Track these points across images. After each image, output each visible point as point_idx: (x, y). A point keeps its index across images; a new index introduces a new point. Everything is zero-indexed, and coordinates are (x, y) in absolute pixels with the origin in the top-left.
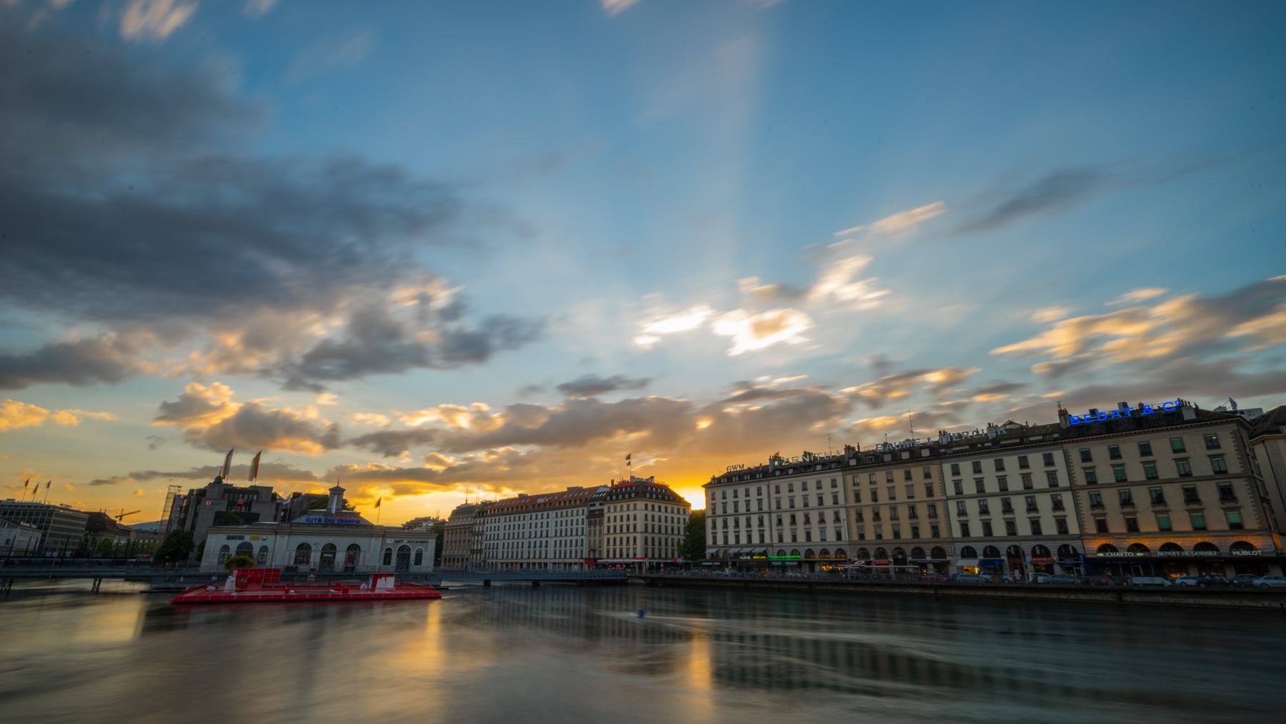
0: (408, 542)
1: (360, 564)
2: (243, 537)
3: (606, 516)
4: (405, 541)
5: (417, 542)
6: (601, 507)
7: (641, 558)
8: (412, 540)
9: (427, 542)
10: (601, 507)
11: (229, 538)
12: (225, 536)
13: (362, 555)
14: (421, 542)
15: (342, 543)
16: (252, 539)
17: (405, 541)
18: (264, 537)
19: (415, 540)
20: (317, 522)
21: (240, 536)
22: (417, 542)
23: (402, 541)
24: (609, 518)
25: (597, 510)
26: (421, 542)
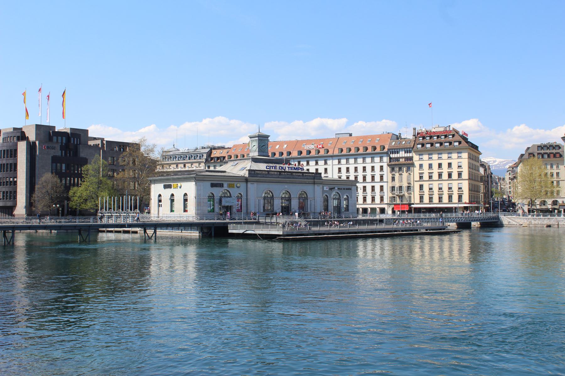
0: (339, 189)
1: (309, 211)
2: (223, 184)
3: (417, 164)
4: (336, 188)
5: (344, 189)
6: (409, 155)
7: (465, 203)
8: (340, 187)
9: (351, 189)
10: (409, 155)
11: (213, 185)
12: (208, 184)
13: (309, 201)
14: (347, 189)
15: (296, 190)
16: (229, 186)
17: (336, 188)
18: (238, 185)
19: (343, 187)
20: (273, 170)
21: (220, 184)
22: (344, 189)
23: (334, 188)
24: (421, 166)
25: (402, 158)
26: (347, 189)
